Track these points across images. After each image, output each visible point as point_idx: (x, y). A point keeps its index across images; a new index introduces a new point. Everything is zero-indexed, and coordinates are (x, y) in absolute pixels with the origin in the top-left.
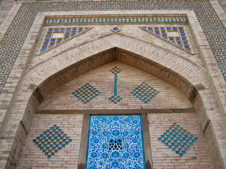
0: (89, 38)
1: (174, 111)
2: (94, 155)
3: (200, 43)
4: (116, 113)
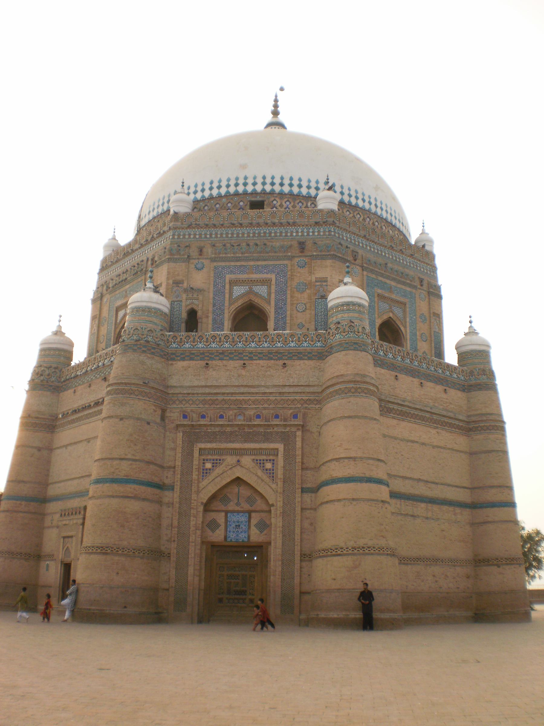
0: (224, 468)
1: (262, 511)
2: (230, 532)
3: (279, 477)
4: (238, 512)
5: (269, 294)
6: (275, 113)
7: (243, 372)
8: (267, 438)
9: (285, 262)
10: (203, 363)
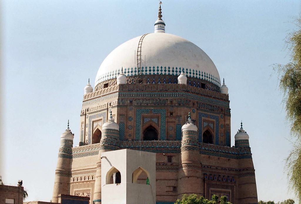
5: (214, 127)
6: (160, 16)
7: (219, 161)
8: (227, 187)
9: (218, 115)
10: (208, 156)
